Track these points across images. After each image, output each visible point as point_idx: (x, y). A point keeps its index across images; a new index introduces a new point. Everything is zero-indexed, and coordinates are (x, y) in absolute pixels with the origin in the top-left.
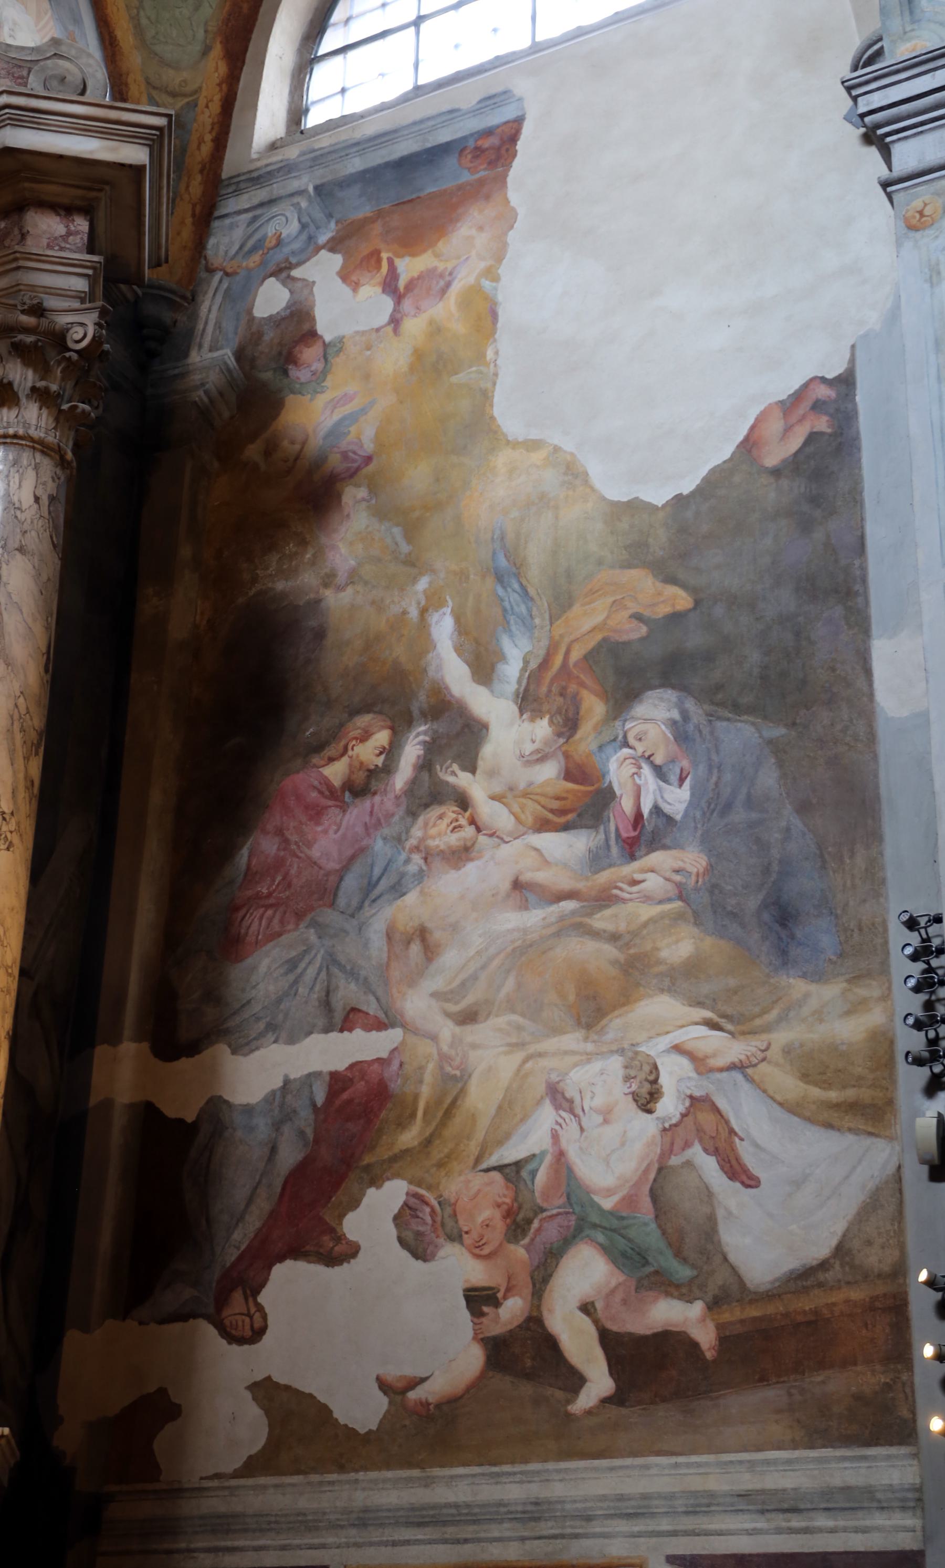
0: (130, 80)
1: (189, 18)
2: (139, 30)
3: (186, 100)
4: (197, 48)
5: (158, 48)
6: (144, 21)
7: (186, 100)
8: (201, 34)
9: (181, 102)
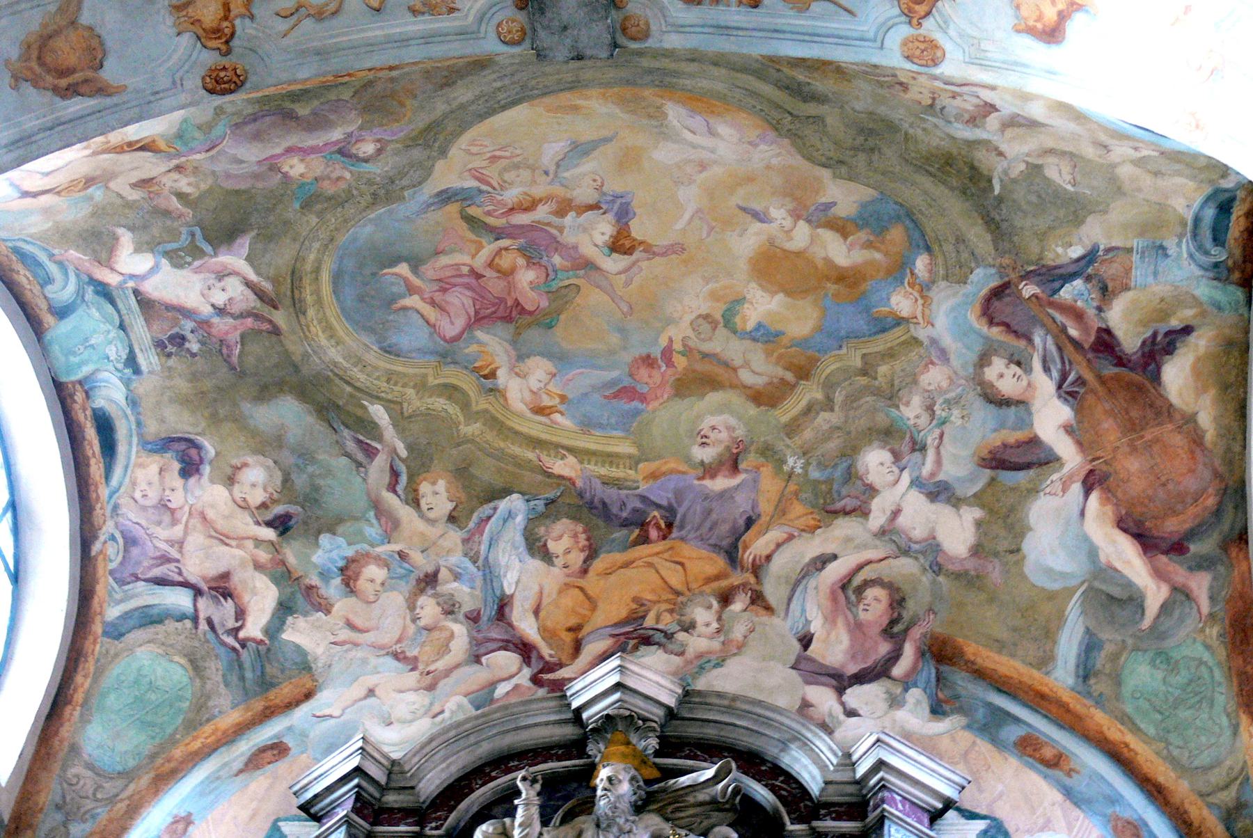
0: (1187, 806)
1: (1210, 718)
2: (1174, 762)
3: (1238, 782)
4: (1228, 733)
5: (1197, 763)
6: (1176, 752)
7: (1238, 782)
8: (1225, 721)
9: (1234, 789)
